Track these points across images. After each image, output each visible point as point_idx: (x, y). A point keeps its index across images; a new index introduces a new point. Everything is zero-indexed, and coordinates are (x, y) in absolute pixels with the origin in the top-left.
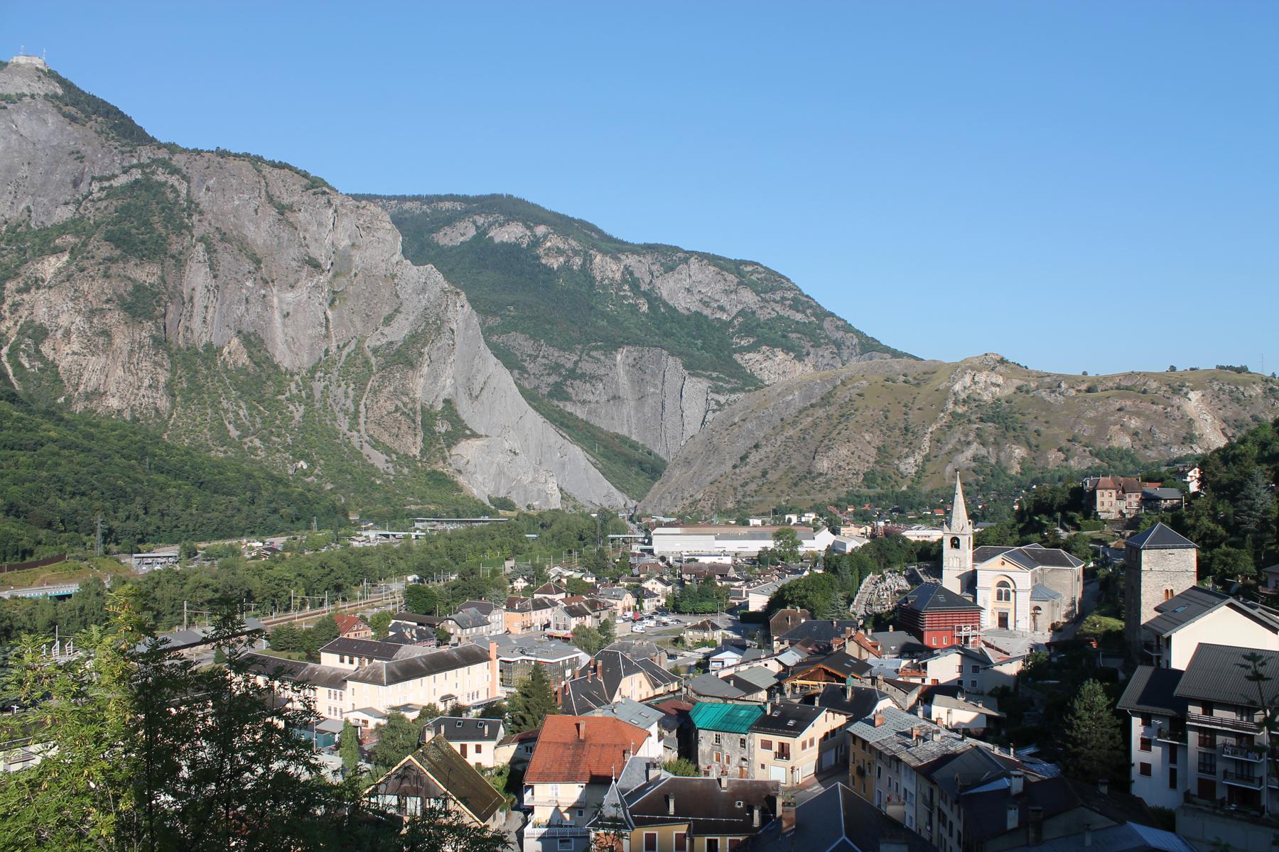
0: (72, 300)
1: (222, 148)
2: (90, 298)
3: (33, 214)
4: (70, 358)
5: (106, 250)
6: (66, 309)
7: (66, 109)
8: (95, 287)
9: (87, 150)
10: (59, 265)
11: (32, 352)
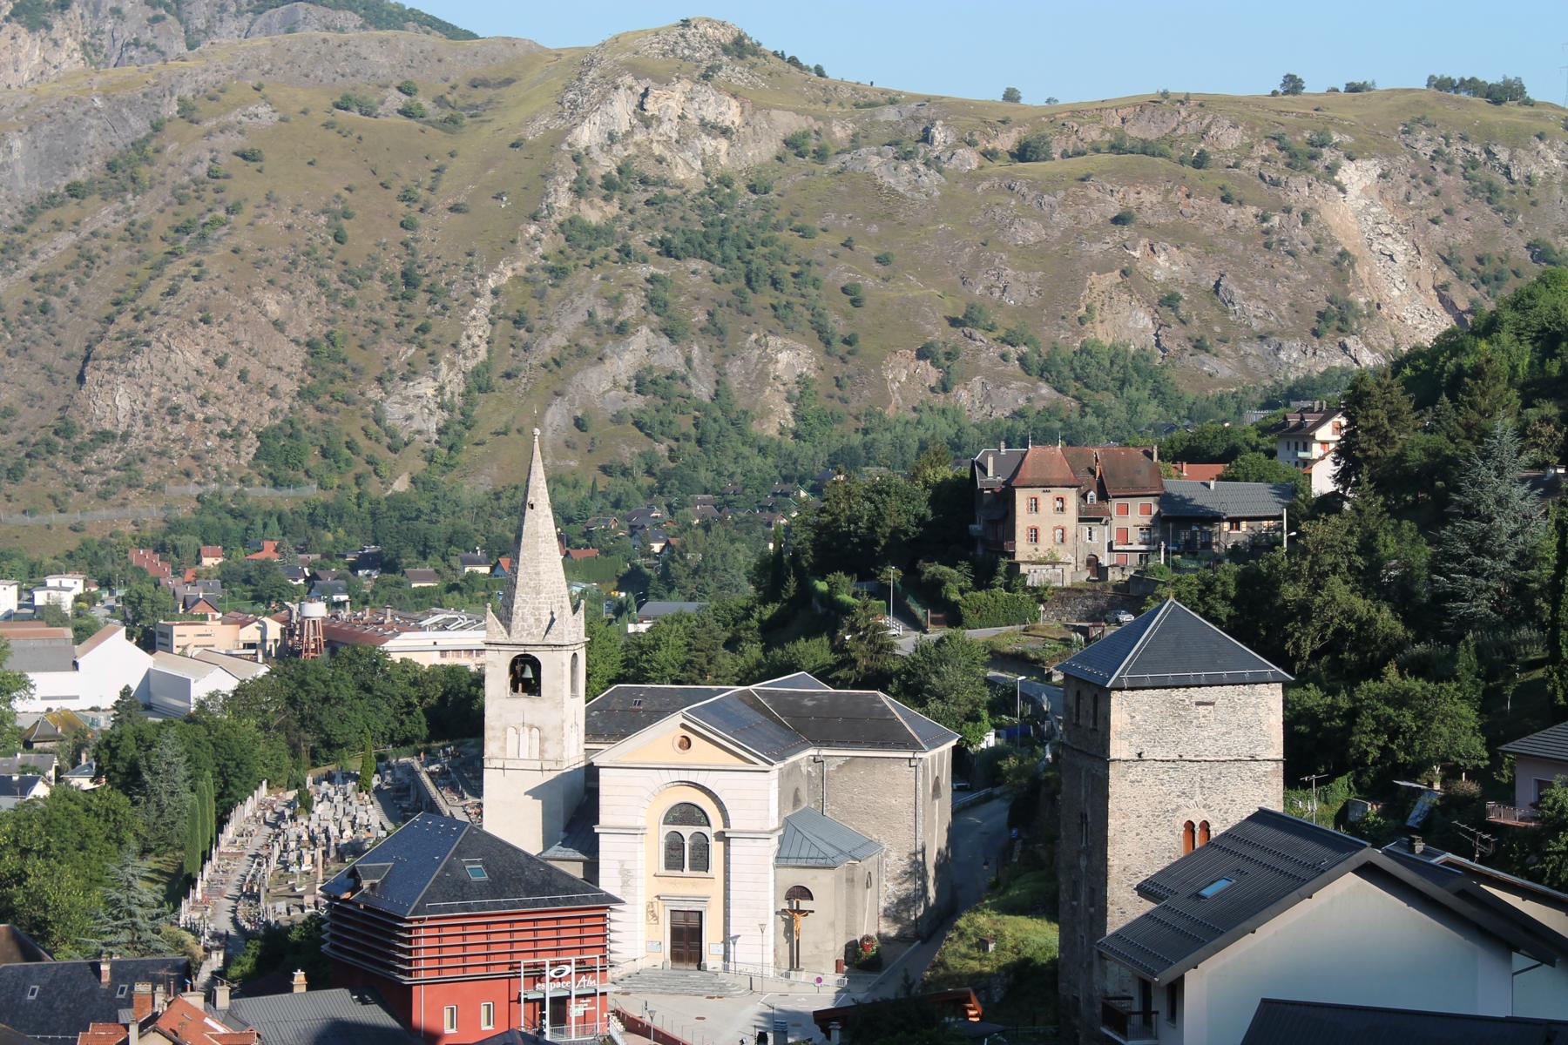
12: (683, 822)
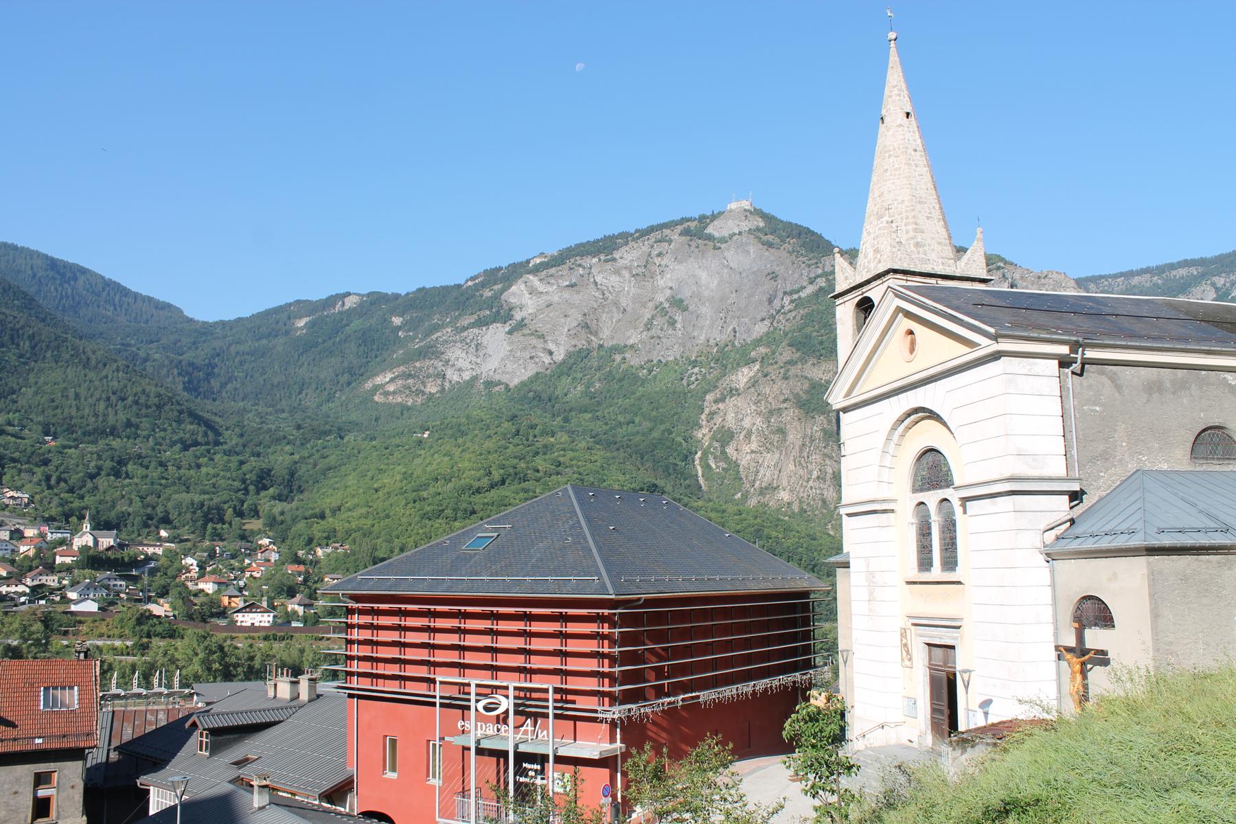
0: (755, 403)
2: (770, 399)
3: (738, 334)
4: (748, 457)
5: (787, 354)
6: (749, 412)
7: (765, 238)
8: (775, 390)
9: (780, 270)
10: (752, 374)
11: (718, 454)
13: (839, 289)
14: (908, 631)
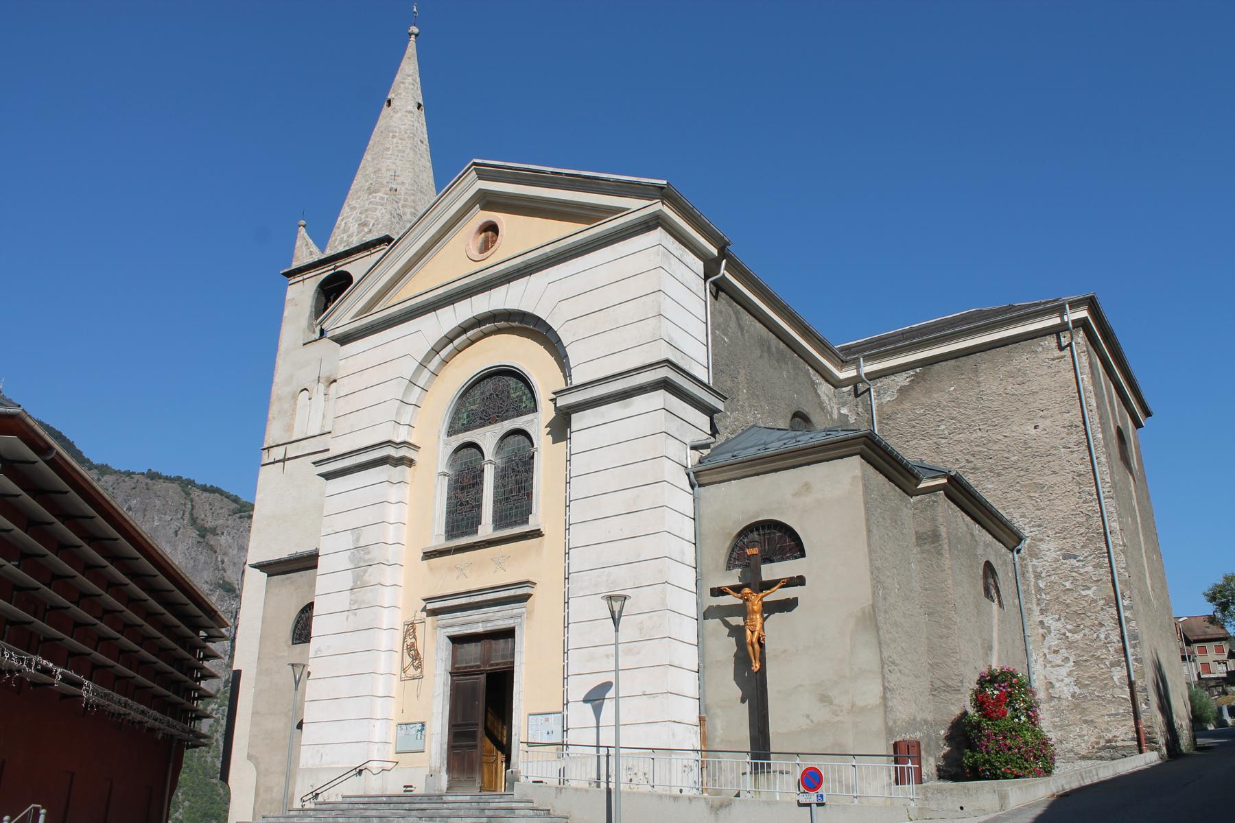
1: (154, 470)
12: (487, 419)
13: (295, 265)
14: (419, 628)
